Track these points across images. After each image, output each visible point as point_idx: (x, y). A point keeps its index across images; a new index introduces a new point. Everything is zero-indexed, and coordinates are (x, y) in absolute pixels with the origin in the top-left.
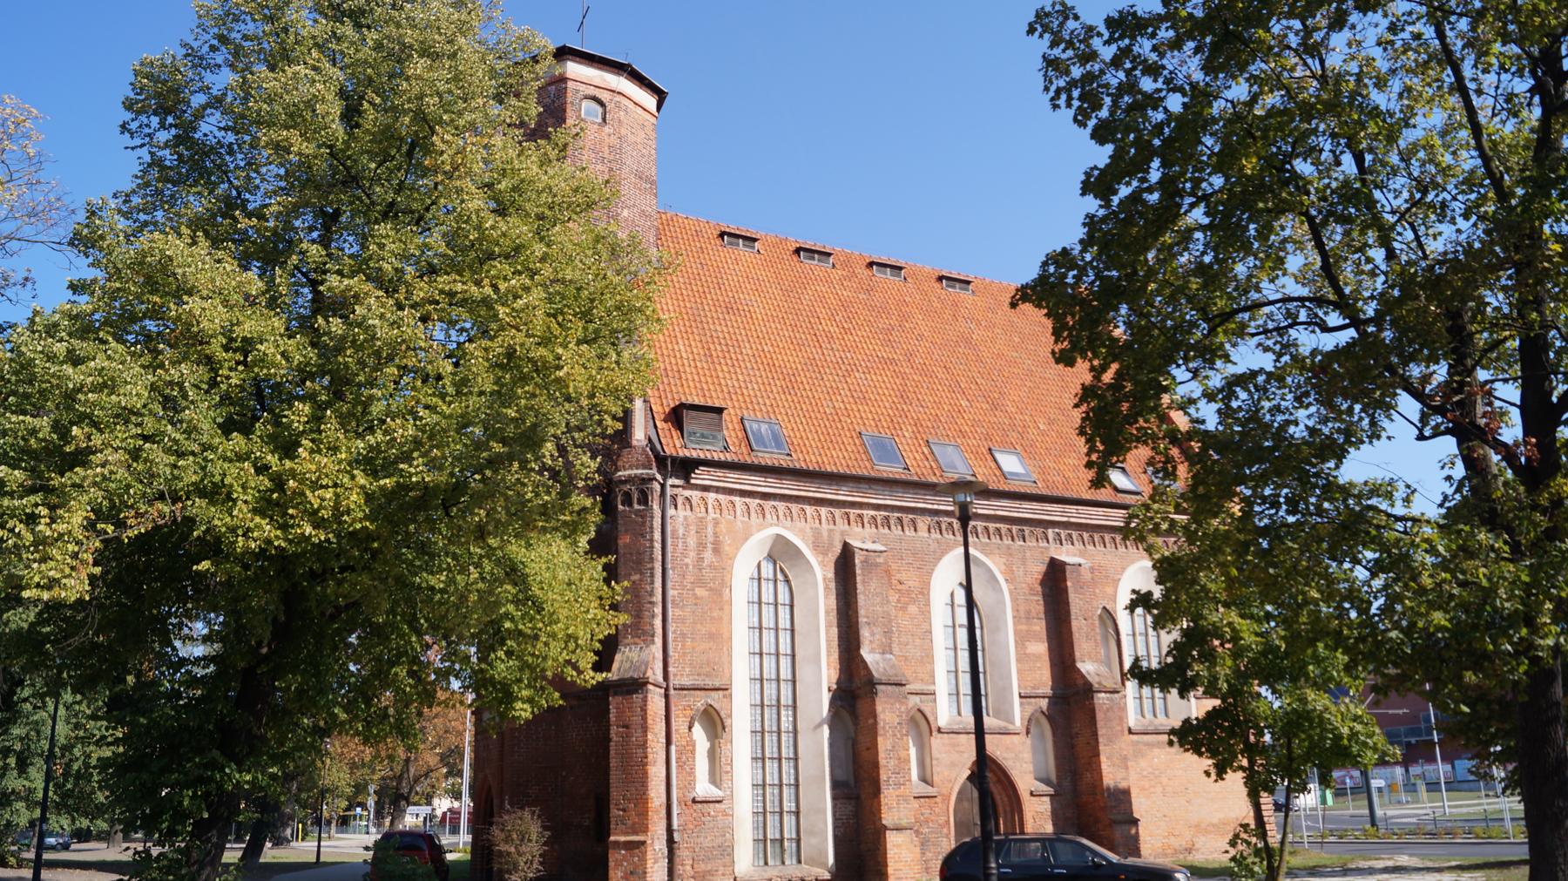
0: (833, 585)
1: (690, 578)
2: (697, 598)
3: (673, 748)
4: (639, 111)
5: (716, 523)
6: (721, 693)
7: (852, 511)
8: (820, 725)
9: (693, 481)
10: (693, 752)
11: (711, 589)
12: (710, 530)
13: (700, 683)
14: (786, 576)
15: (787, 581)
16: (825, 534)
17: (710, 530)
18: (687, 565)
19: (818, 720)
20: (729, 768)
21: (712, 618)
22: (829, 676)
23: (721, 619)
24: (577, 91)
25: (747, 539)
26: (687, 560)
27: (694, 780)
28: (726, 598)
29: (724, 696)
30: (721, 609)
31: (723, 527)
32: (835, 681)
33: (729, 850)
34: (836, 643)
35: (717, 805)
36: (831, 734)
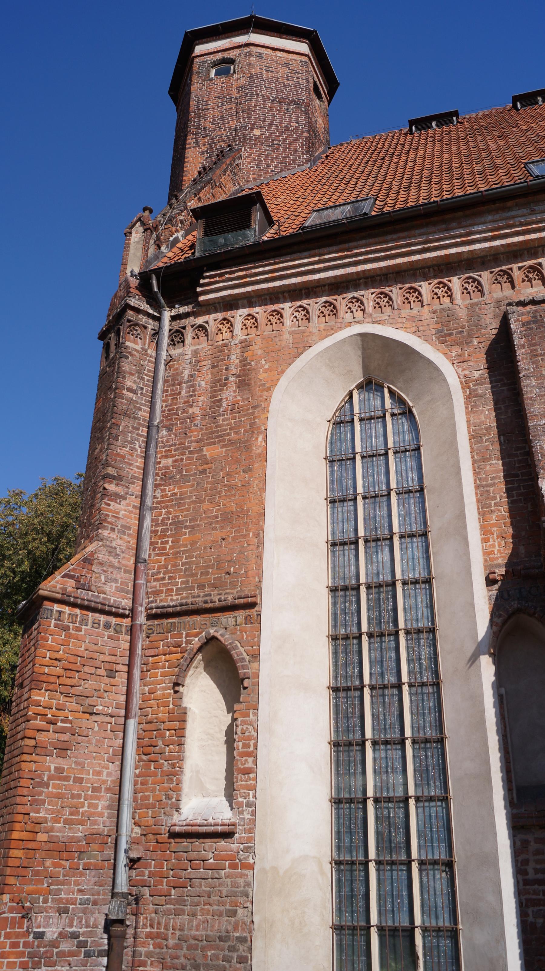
0: (486, 389)
1: (195, 435)
2: (206, 462)
3: (132, 724)
4: (280, 54)
5: (245, 345)
6: (241, 615)
7: (515, 266)
8: (474, 658)
9: (201, 298)
10: (180, 733)
11: (231, 443)
12: (235, 358)
13: (200, 603)
14: (401, 402)
15: (408, 413)
16: (462, 313)
17: (235, 358)
18: (192, 418)
19: (470, 649)
20: (250, 763)
21: (231, 487)
22: (487, 554)
23: (246, 485)
24: (204, 62)
25: (299, 354)
26: (195, 410)
27: (178, 789)
28: (256, 450)
29: (248, 620)
30: (248, 470)
31: (257, 349)
32: (502, 561)
33: (242, 947)
34: (501, 485)
35: (222, 843)
36: (498, 674)
